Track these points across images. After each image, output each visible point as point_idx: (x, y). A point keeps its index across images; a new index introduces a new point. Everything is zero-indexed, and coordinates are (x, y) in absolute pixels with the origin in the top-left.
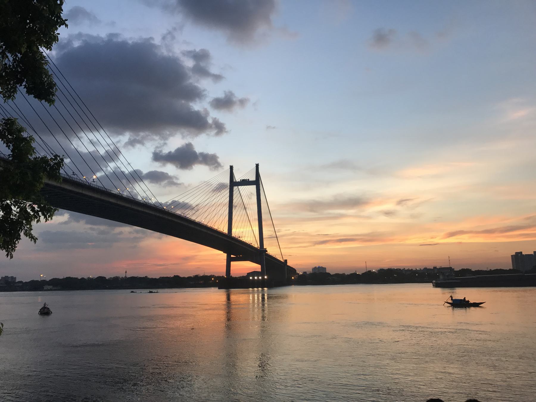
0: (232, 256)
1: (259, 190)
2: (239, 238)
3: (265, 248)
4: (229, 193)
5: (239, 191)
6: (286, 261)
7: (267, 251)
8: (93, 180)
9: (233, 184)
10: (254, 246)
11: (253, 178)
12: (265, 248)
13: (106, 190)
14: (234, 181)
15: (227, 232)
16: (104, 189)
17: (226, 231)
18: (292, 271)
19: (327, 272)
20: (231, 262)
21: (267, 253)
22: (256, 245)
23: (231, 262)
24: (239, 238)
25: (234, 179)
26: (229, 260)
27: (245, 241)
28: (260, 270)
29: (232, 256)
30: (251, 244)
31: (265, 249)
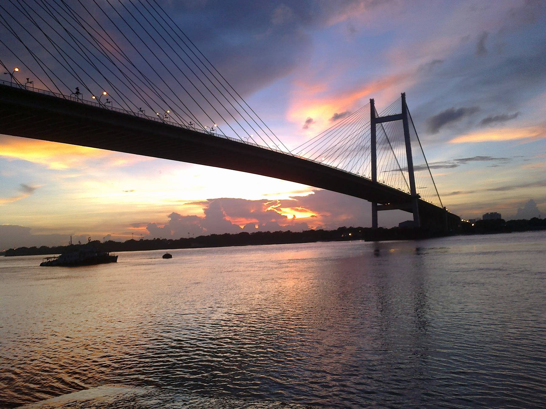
0: (378, 204)
1: (407, 124)
2: (384, 183)
3: (417, 193)
4: (370, 131)
5: (382, 126)
6: (445, 207)
7: (420, 197)
8: (212, 128)
9: (375, 120)
10: (404, 191)
11: (399, 111)
12: (417, 193)
13: (226, 138)
14: (376, 115)
15: (371, 176)
16: (224, 137)
17: (368, 175)
18: (455, 219)
19: (502, 218)
20: (378, 212)
21: (420, 199)
22: (406, 189)
23: (378, 212)
24: (384, 183)
25: (376, 113)
26: (375, 210)
27: (391, 186)
28: (412, 219)
29: (378, 204)
30: (400, 189)
31: (418, 194)
